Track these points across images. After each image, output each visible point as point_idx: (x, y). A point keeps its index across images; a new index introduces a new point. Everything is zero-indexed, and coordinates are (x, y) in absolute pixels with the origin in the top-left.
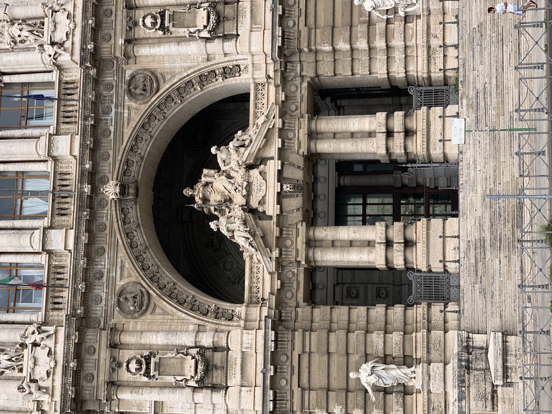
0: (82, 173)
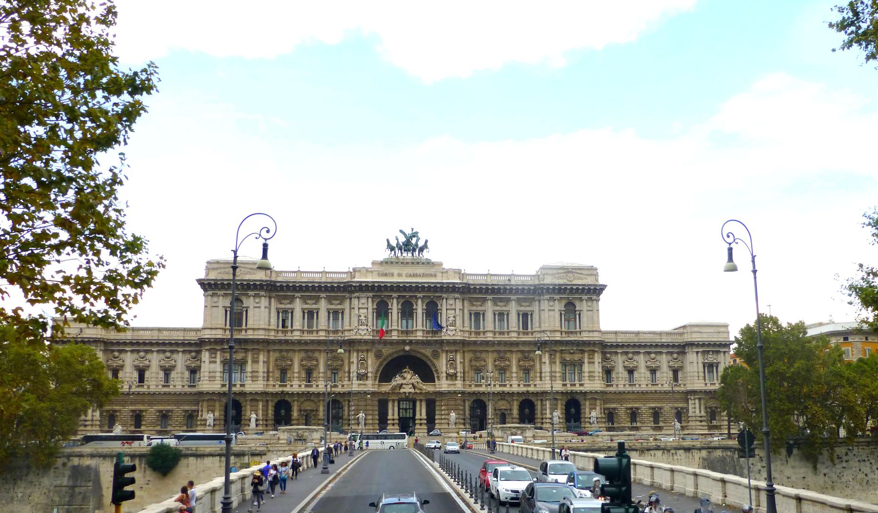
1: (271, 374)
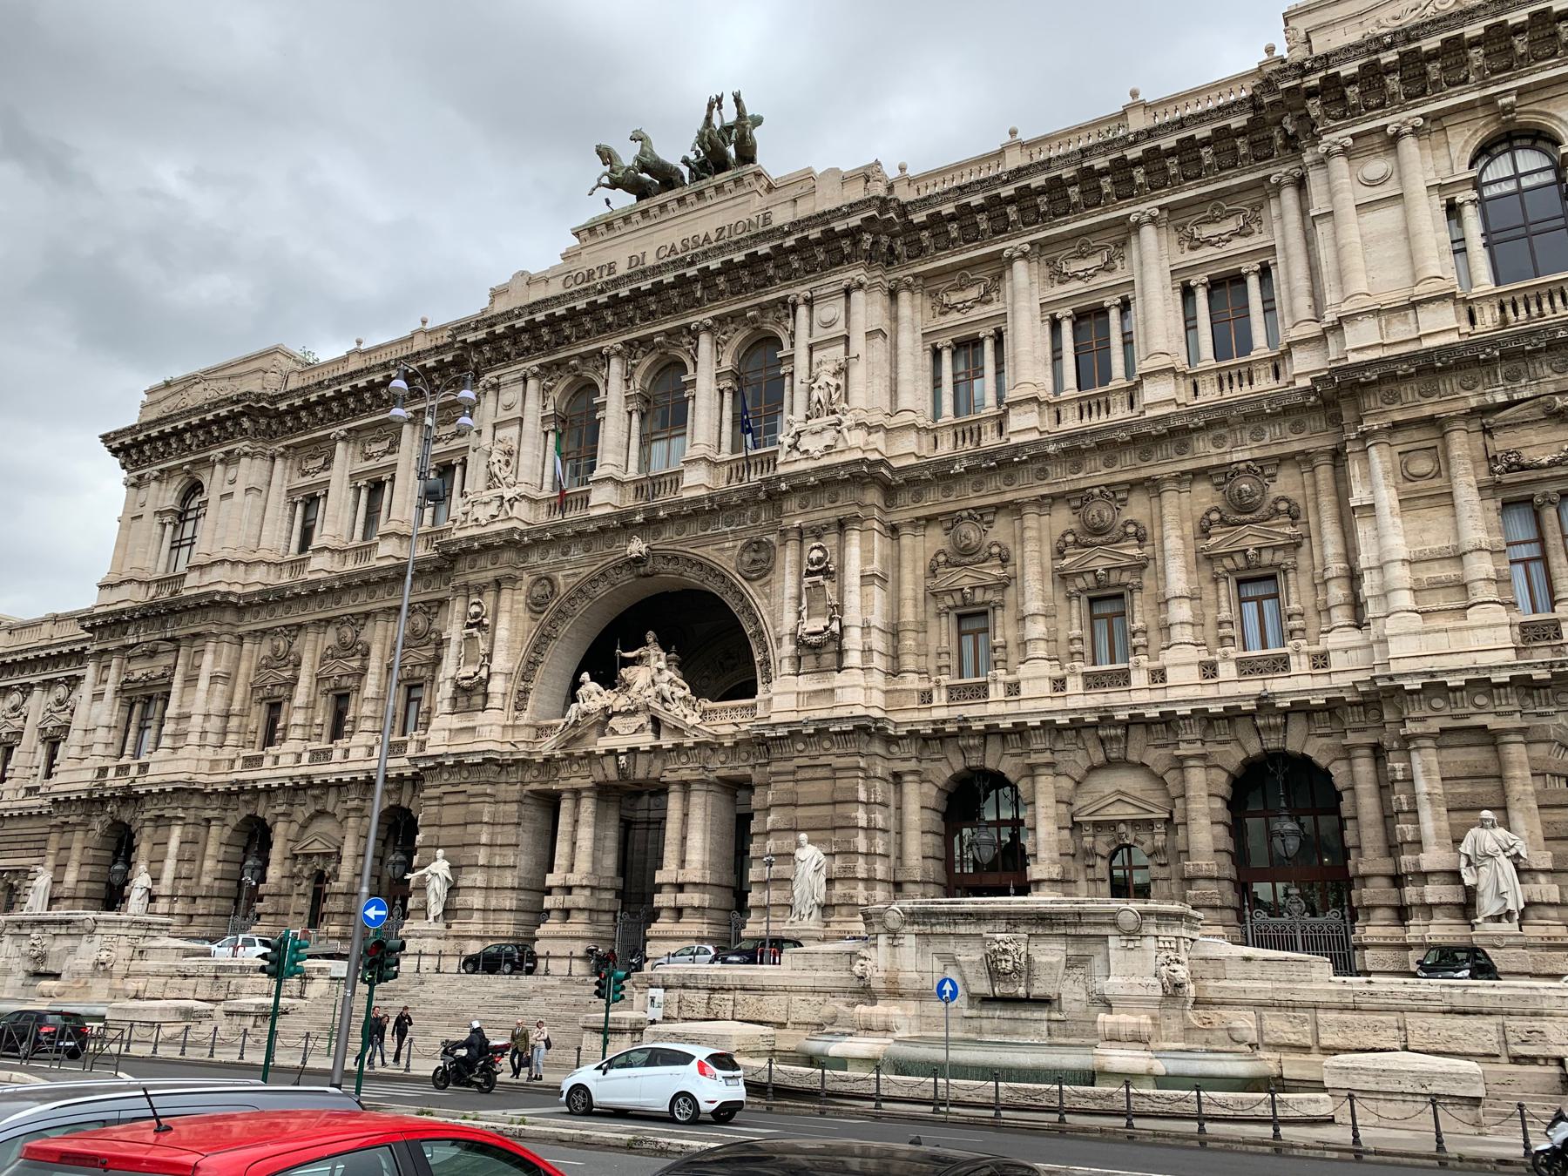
0: (655, 509)
1: (234, 723)
